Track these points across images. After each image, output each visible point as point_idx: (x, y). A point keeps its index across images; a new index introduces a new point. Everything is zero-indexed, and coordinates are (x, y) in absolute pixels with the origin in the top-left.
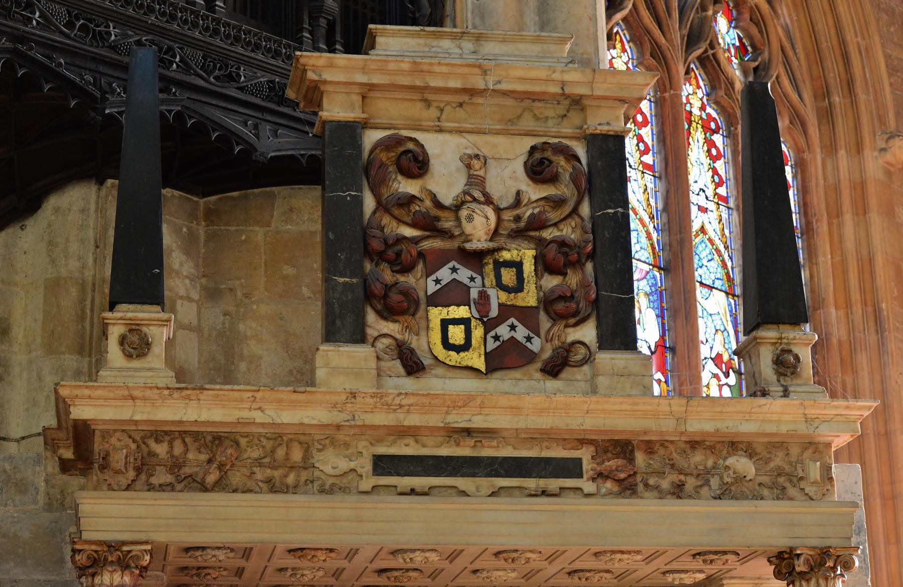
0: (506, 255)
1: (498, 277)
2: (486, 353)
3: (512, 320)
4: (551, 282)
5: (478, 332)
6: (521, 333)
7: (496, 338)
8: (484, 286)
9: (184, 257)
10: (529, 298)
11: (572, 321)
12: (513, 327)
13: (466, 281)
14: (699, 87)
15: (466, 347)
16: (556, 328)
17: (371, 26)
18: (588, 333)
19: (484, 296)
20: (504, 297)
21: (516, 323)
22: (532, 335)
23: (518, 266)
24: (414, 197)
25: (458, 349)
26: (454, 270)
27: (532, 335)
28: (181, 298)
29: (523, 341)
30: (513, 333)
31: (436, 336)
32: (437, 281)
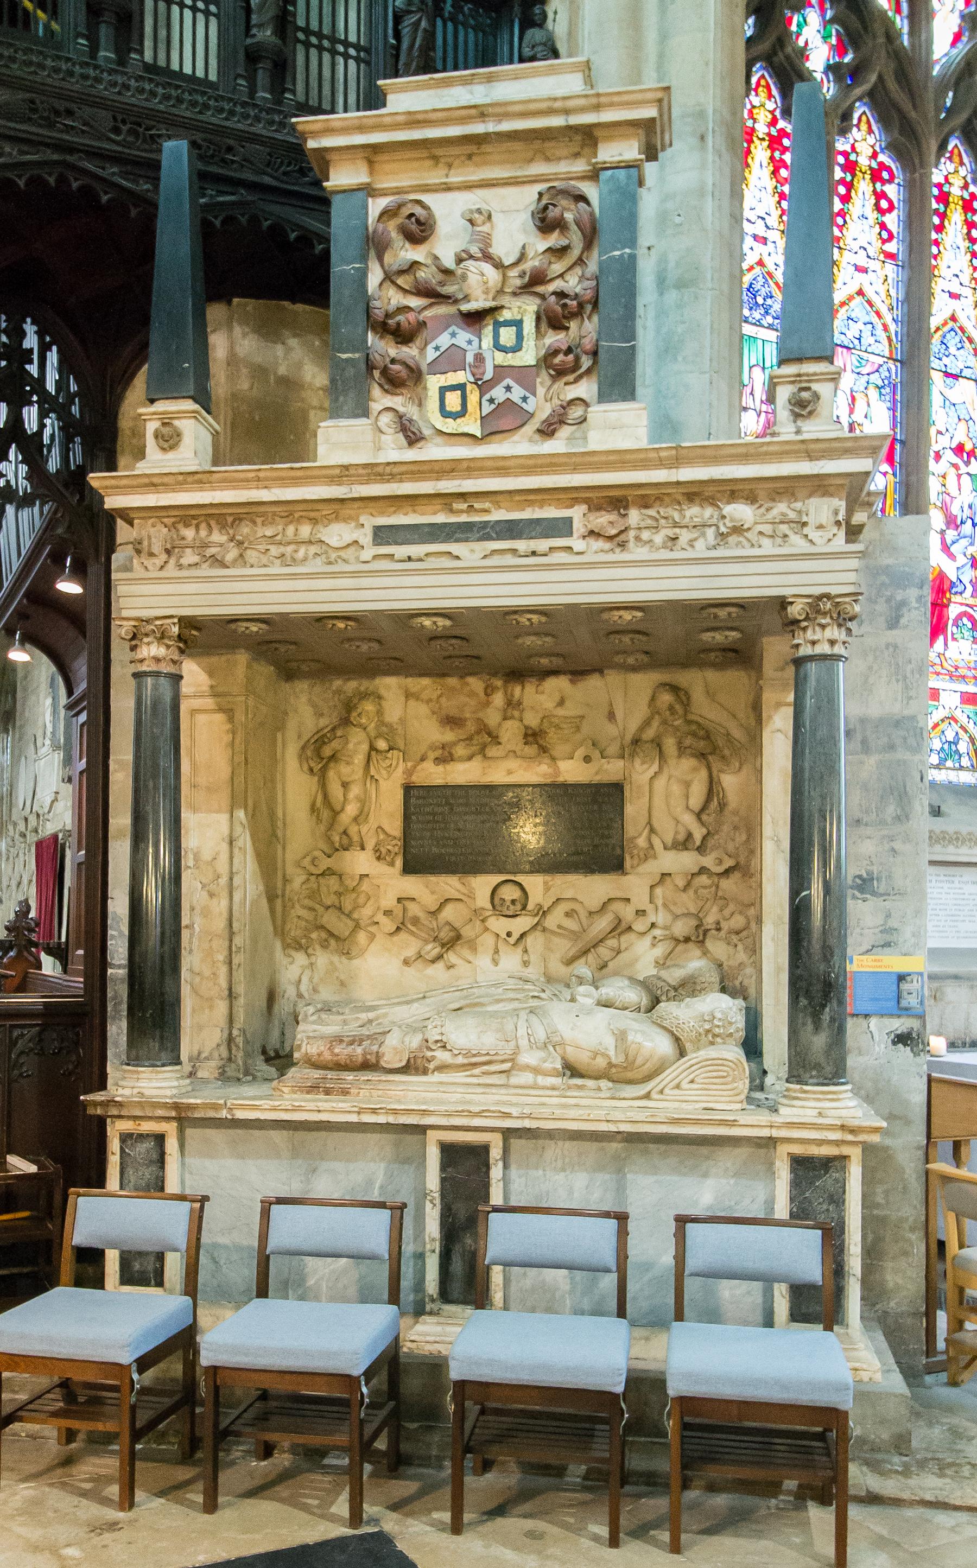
0: (506, 315)
1: (496, 336)
2: (482, 418)
3: (508, 381)
4: (553, 339)
5: (473, 396)
6: (517, 393)
7: (491, 401)
8: (480, 347)
9: (316, 369)
10: (528, 356)
11: (571, 378)
12: (508, 388)
13: (464, 345)
14: (962, 164)
15: (463, 413)
16: (556, 386)
17: (380, 82)
18: (585, 389)
19: (479, 358)
20: (500, 358)
21: (512, 383)
22: (528, 395)
23: (518, 324)
24: (416, 263)
25: (455, 416)
26: (453, 335)
27: (528, 395)
28: (315, 408)
29: (519, 402)
30: (508, 395)
31: (433, 403)
32: (437, 348)
